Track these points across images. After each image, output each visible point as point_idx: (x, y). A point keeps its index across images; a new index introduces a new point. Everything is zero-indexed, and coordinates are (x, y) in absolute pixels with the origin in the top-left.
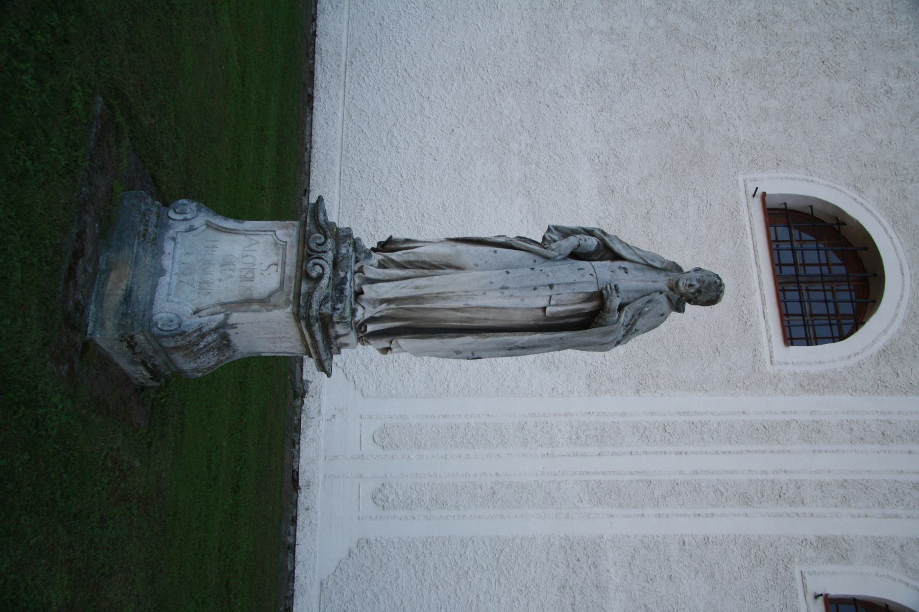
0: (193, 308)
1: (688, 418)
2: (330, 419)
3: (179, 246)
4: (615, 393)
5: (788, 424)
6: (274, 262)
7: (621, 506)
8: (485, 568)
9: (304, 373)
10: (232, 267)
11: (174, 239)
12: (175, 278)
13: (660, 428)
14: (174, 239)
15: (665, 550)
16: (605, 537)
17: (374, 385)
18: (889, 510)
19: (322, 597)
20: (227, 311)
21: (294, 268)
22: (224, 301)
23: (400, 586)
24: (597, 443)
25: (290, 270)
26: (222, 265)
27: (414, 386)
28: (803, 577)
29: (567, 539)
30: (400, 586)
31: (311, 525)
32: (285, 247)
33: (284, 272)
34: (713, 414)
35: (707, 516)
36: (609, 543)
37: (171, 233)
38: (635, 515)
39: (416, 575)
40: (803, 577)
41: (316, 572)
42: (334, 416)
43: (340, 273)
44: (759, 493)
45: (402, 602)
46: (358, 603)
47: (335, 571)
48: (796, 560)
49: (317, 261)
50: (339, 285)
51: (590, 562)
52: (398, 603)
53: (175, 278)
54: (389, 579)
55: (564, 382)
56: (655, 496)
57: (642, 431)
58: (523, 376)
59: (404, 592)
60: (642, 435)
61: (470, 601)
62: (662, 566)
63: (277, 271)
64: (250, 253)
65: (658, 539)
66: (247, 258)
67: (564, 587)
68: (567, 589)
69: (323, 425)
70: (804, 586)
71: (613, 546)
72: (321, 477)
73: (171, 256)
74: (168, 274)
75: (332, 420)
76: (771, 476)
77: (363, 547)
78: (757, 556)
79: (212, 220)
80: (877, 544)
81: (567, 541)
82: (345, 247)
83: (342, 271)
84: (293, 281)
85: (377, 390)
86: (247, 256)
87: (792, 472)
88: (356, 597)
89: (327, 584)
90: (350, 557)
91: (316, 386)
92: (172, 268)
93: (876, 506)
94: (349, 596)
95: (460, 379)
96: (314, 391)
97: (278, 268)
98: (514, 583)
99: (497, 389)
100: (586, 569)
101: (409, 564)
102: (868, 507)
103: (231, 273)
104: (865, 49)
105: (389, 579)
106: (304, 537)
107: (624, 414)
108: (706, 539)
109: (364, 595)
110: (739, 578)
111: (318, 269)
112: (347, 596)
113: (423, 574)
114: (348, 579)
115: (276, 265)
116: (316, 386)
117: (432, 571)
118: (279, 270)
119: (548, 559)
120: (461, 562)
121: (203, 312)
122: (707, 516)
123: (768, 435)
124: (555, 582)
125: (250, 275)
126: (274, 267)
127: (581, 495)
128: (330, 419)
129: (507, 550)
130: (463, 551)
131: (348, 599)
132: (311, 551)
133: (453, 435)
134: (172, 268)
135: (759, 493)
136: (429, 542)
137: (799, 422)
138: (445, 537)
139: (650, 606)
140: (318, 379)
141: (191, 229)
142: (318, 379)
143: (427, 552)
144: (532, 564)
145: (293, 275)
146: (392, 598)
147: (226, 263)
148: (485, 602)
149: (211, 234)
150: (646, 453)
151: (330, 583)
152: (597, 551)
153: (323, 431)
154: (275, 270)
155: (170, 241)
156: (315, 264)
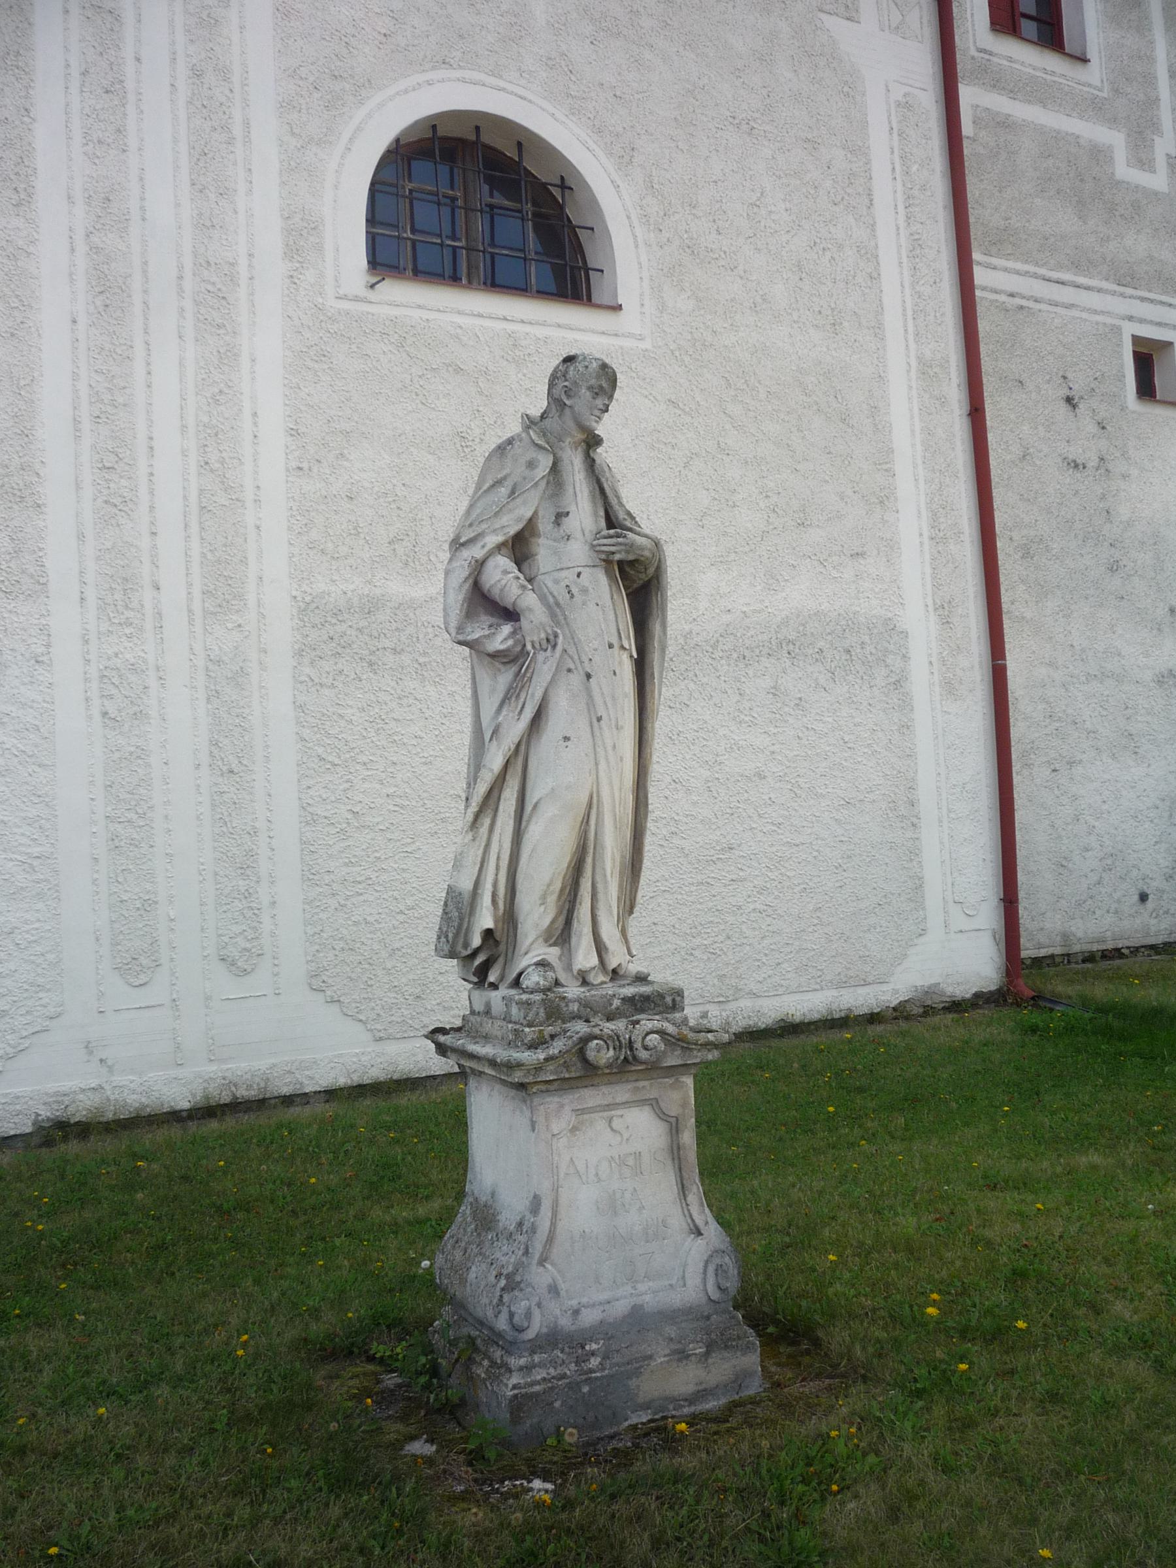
0: (689, 1240)
1: (86, 425)
2: (109, 1067)
3: (584, 1300)
4: (40, 549)
5: (96, 250)
6: (607, 1125)
7: (244, 561)
8: (347, 785)
9: (18, 1132)
10: (618, 1195)
11: (576, 1312)
12: (641, 1287)
13: (106, 475)
14: (576, 1312)
15: (311, 501)
16: (294, 593)
17: (41, 995)
18: (238, 131)
19: (398, 1036)
20: (695, 1182)
21: (617, 1088)
22: (676, 1191)
23: (377, 917)
24: (138, 591)
25: (621, 1092)
26: (615, 1213)
27: (39, 920)
28: (345, 297)
29: (300, 653)
30: (377, 917)
31: (293, 1070)
32: (579, 1112)
33: (627, 1102)
34: (75, 377)
35: (255, 424)
36: (305, 588)
37: (565, 1322)
38: (257, 541)
39: (361, 894)
40: (345, 297)
41: (362, 1050)
42: (101, 1060)
43: (614, 1006)
44: (218, 332)
45: (401, 912)
46: (404, 980)
47: (361, 1021)
48: (320, 300)
49: (638, 1045)
50: (636, 1005)
51: (334, 621)
52: (401, 918)
53: (641, 1287)
54: (369, 936)
55: (24, 640)
56: (227, 503)
57: (115, 510)
58: (13, 718)
59: (387, 910)
60: (120, 510)
61: (397, 809)
62: (335, 508)
63: (622, 1116)
64: (592, 1171)
65: (294, 508)
66: (600, 1173)
67: (371, 664)
68: (373, 658)
69: (118, 1079)
70: (356, 299)
71: (308, 582)
72: (214, 1067)
73: (607, 1307)
74: (638, 1301)
75: (110, 1063)
76: (188, 304)
77: (324, 982)
78: (315, 358)
79: (537, 1256)
80: (292, 170)
81: (304, 653)
82: (567, 1006)
83: (611, 1005)
84: (641, 1084)
85: (49, 990)
86: (597, 1175)
87: (181, 268)
88: (396, 984)
89: (380, 1031)
90: (339, 1001)
91: (45, 1104)
92: (625, 1297)
93: (233, 149)
94: (394, 995)
95: (23, 835)
96: (55, 1106)
97: (617, 1116)
98: (369, 740)
99: (39, 766)
100: (344, 627)
101: (345, 905)
102: (235, 164)
103: (628, 1195)
104: (592, 43)
105: (369, 936)
106: (312, 1078)
107: (81, 537)
108: (294, 433)
109: (393, 971)
110: (348, 395)
111: (654, 1039)
112: (395, 998)
113: (360, 883)
114: (370, 999)
115: (610, 1120)
116: (45, 1104)
117: (354, 869)
118: (619, 1112)
119: (333, 686)
120: (339, 823)
121: (698, 1221)
122: (255, 424)
123: (117, 290)
124: (365, 677)
125: (631, 1162)
126: (615, 1124)
127: (230, 625)
128: (109, 1067)
129: (320, 750)
130: (325, 820)
131: (399, 997)
132: (332, 1065)
133: (131, 844)
134: (625, 1297)
135: (218, 332)
136: (311, 877)
137: (92, 229)
138: (302, 850)
139: (391, 536)
140: (30, 1103)
141: (554, 1290)
142: (30, 1103)
143: (327, 879)
144: (340, 712)
145: (630, 1086)
146: (395, 928)
147: (612, 1206)
148: (396, 786)
149: (556, 1252)
150: (152, 508)
151: (379, 1027)
152: (317, 607)
153: (131, 1077)
154: (620, 1120)
155: (580, 1318)
156: (646, 1048)
